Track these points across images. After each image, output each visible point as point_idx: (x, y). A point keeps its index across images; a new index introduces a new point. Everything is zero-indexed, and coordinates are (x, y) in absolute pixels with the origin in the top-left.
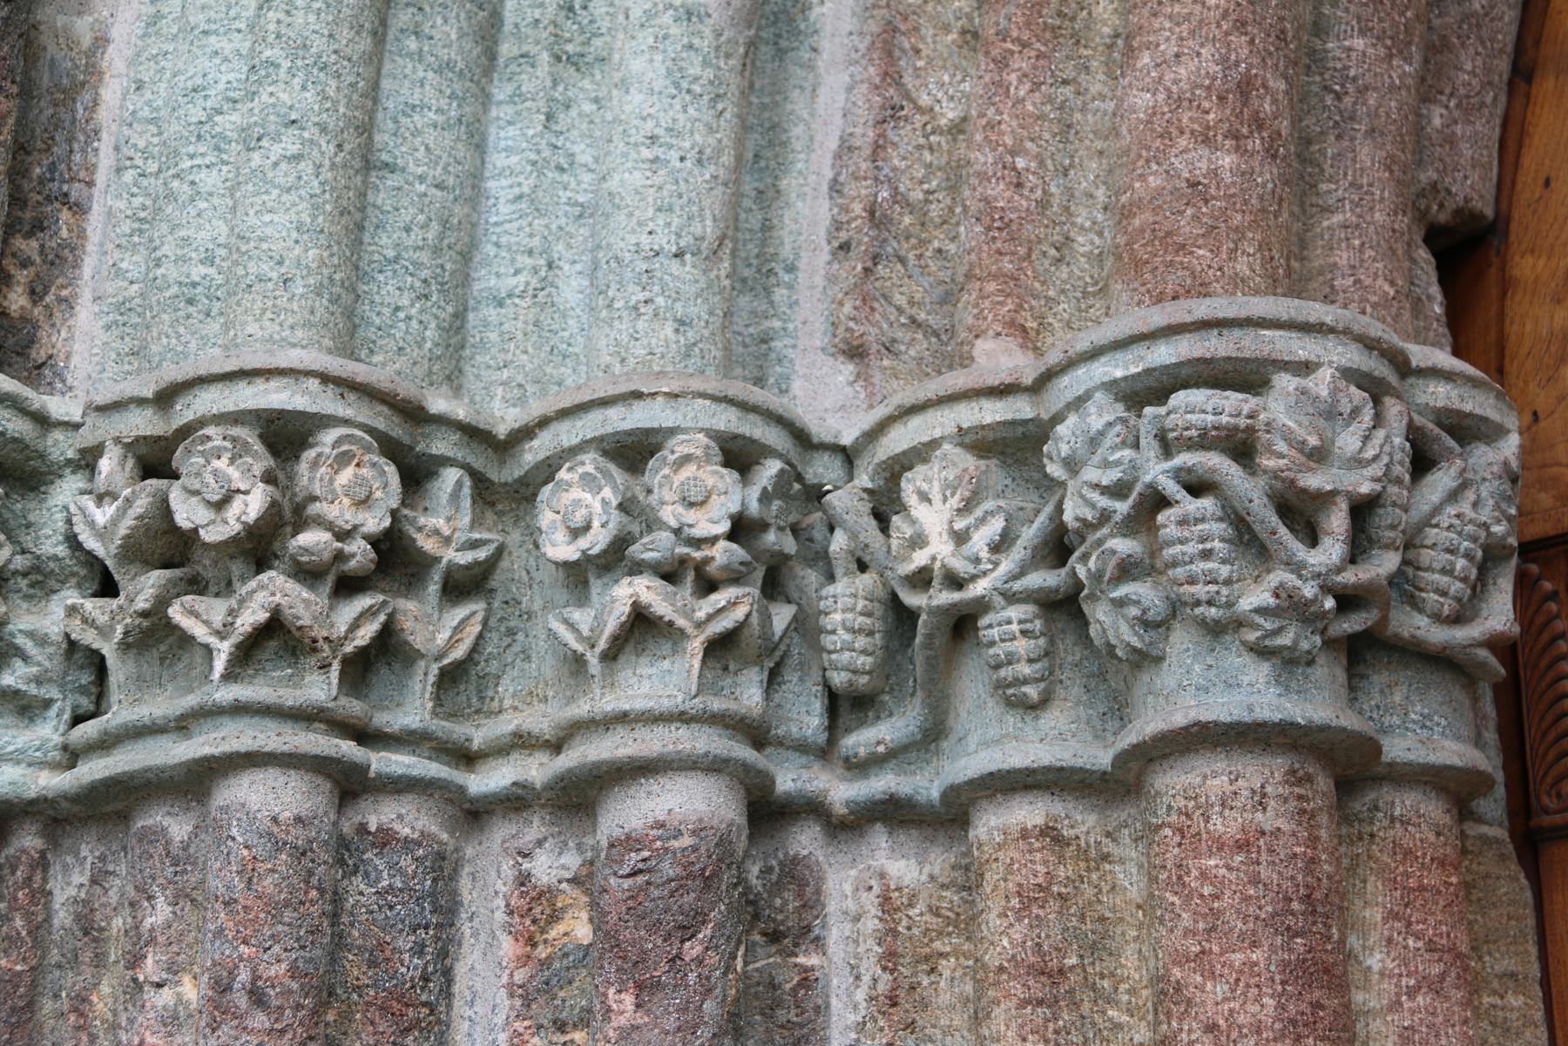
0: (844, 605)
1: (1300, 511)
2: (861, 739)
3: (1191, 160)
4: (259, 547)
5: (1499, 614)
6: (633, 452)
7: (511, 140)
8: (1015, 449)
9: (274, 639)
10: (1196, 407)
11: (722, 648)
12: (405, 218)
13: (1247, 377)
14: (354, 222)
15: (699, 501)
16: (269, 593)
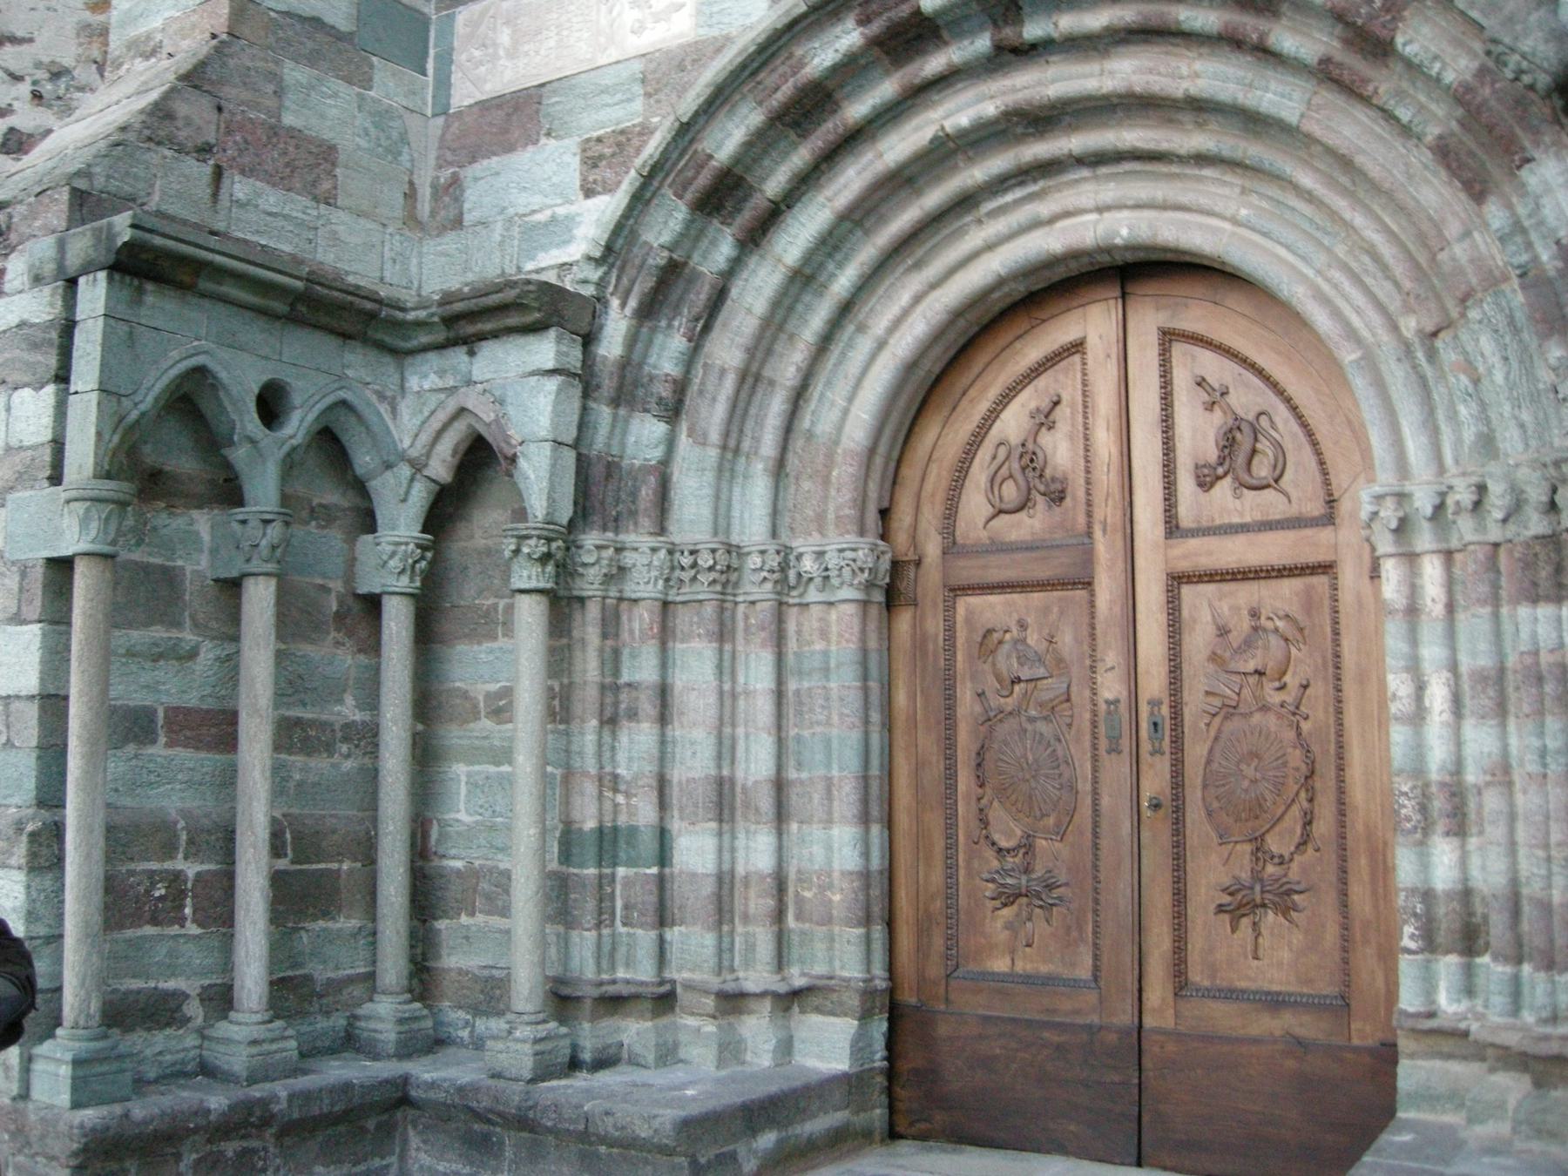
0: (792, 574)
1: (862, 570)
2: (794, 593)
3: (847, 511)
4: (711, 569)
5: (887, 580)
6: (763, 552)
7: (737, 491)
8: (820, 555)
9: (714, 581)
10: (849, 554)
11: (776, 582)
12: (722, 511)
13: (854, 550)
14: (716, 509)
15: (773, 561)
16: (713, 575)
